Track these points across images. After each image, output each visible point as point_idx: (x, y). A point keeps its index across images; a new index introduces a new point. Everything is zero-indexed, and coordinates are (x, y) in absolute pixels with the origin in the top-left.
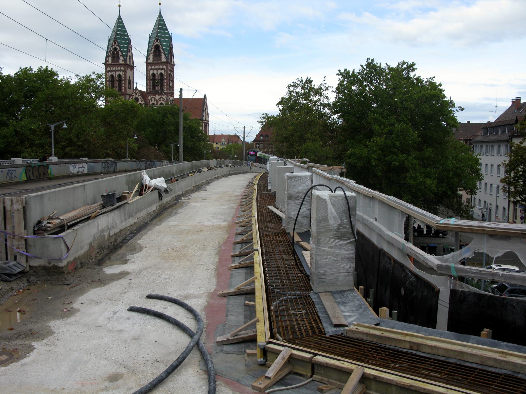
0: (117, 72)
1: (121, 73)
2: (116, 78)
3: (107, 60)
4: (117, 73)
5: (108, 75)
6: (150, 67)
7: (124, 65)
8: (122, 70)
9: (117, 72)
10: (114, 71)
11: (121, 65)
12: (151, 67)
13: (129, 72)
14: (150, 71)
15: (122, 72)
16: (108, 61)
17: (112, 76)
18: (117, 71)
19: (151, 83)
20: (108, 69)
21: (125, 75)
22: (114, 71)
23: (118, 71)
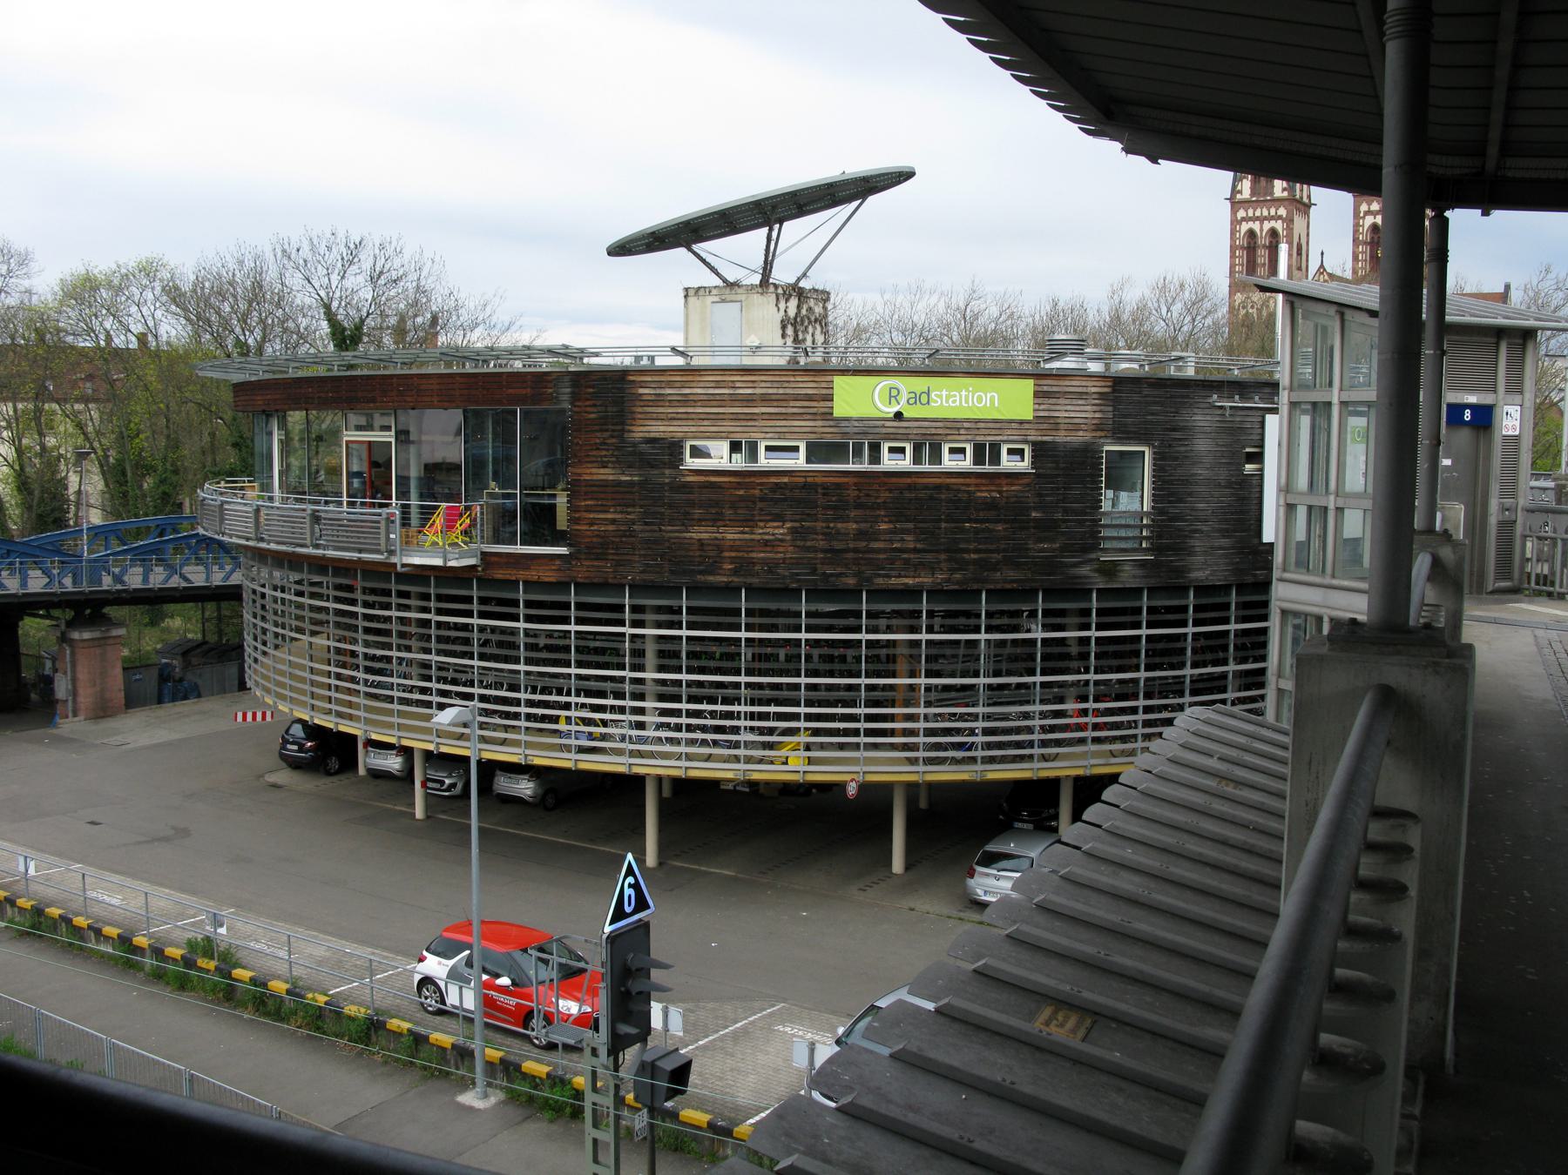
0: (1266, 222)
1: (1279, 225)
2: (1263, 240)
3: (1239, 188)
4: (1267, 226)
5: (1240, 231)
6: (1364, 207)
7: (1286, 203)
8: (1280, 217)
9: (1266, 222)
10: (1257, 219)
11: (1280, 201)
12: (1369, 205)
13: (1299, 222)
14: (1364, 218)
15: (1280, 222)
16: (1240, 192)
17: (1251, 234)
18: (1265, 218)
19: (1366, 252)
20: (1241, 214)
21: (1290, 229)
22: (1257, 219)
23: (1269, 218)
